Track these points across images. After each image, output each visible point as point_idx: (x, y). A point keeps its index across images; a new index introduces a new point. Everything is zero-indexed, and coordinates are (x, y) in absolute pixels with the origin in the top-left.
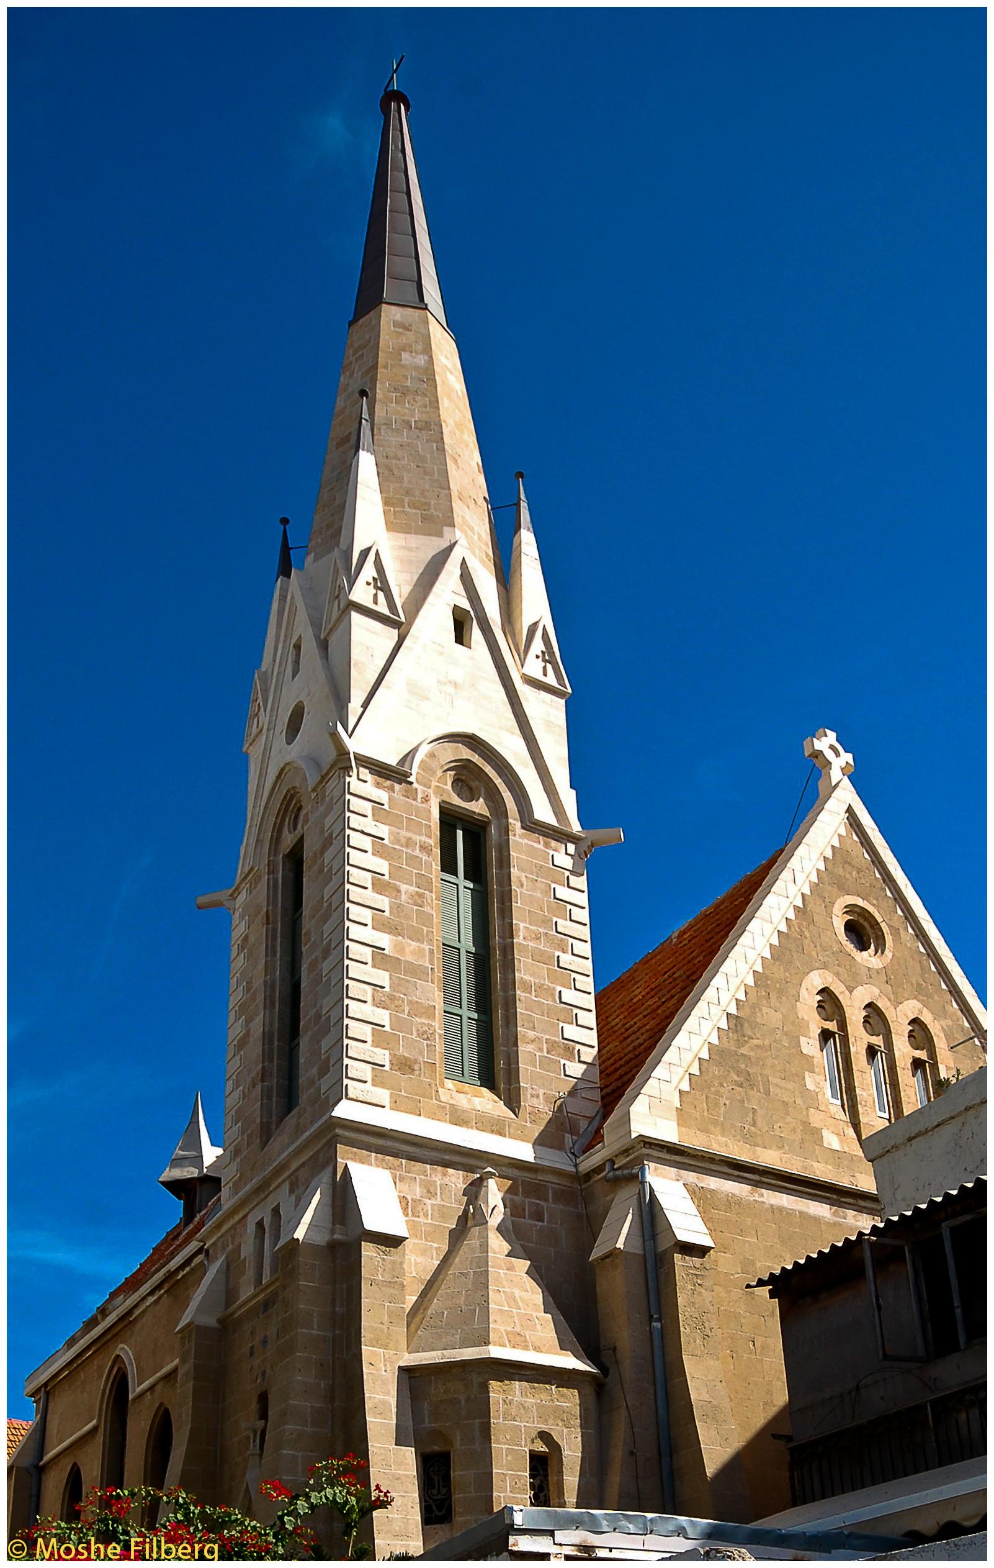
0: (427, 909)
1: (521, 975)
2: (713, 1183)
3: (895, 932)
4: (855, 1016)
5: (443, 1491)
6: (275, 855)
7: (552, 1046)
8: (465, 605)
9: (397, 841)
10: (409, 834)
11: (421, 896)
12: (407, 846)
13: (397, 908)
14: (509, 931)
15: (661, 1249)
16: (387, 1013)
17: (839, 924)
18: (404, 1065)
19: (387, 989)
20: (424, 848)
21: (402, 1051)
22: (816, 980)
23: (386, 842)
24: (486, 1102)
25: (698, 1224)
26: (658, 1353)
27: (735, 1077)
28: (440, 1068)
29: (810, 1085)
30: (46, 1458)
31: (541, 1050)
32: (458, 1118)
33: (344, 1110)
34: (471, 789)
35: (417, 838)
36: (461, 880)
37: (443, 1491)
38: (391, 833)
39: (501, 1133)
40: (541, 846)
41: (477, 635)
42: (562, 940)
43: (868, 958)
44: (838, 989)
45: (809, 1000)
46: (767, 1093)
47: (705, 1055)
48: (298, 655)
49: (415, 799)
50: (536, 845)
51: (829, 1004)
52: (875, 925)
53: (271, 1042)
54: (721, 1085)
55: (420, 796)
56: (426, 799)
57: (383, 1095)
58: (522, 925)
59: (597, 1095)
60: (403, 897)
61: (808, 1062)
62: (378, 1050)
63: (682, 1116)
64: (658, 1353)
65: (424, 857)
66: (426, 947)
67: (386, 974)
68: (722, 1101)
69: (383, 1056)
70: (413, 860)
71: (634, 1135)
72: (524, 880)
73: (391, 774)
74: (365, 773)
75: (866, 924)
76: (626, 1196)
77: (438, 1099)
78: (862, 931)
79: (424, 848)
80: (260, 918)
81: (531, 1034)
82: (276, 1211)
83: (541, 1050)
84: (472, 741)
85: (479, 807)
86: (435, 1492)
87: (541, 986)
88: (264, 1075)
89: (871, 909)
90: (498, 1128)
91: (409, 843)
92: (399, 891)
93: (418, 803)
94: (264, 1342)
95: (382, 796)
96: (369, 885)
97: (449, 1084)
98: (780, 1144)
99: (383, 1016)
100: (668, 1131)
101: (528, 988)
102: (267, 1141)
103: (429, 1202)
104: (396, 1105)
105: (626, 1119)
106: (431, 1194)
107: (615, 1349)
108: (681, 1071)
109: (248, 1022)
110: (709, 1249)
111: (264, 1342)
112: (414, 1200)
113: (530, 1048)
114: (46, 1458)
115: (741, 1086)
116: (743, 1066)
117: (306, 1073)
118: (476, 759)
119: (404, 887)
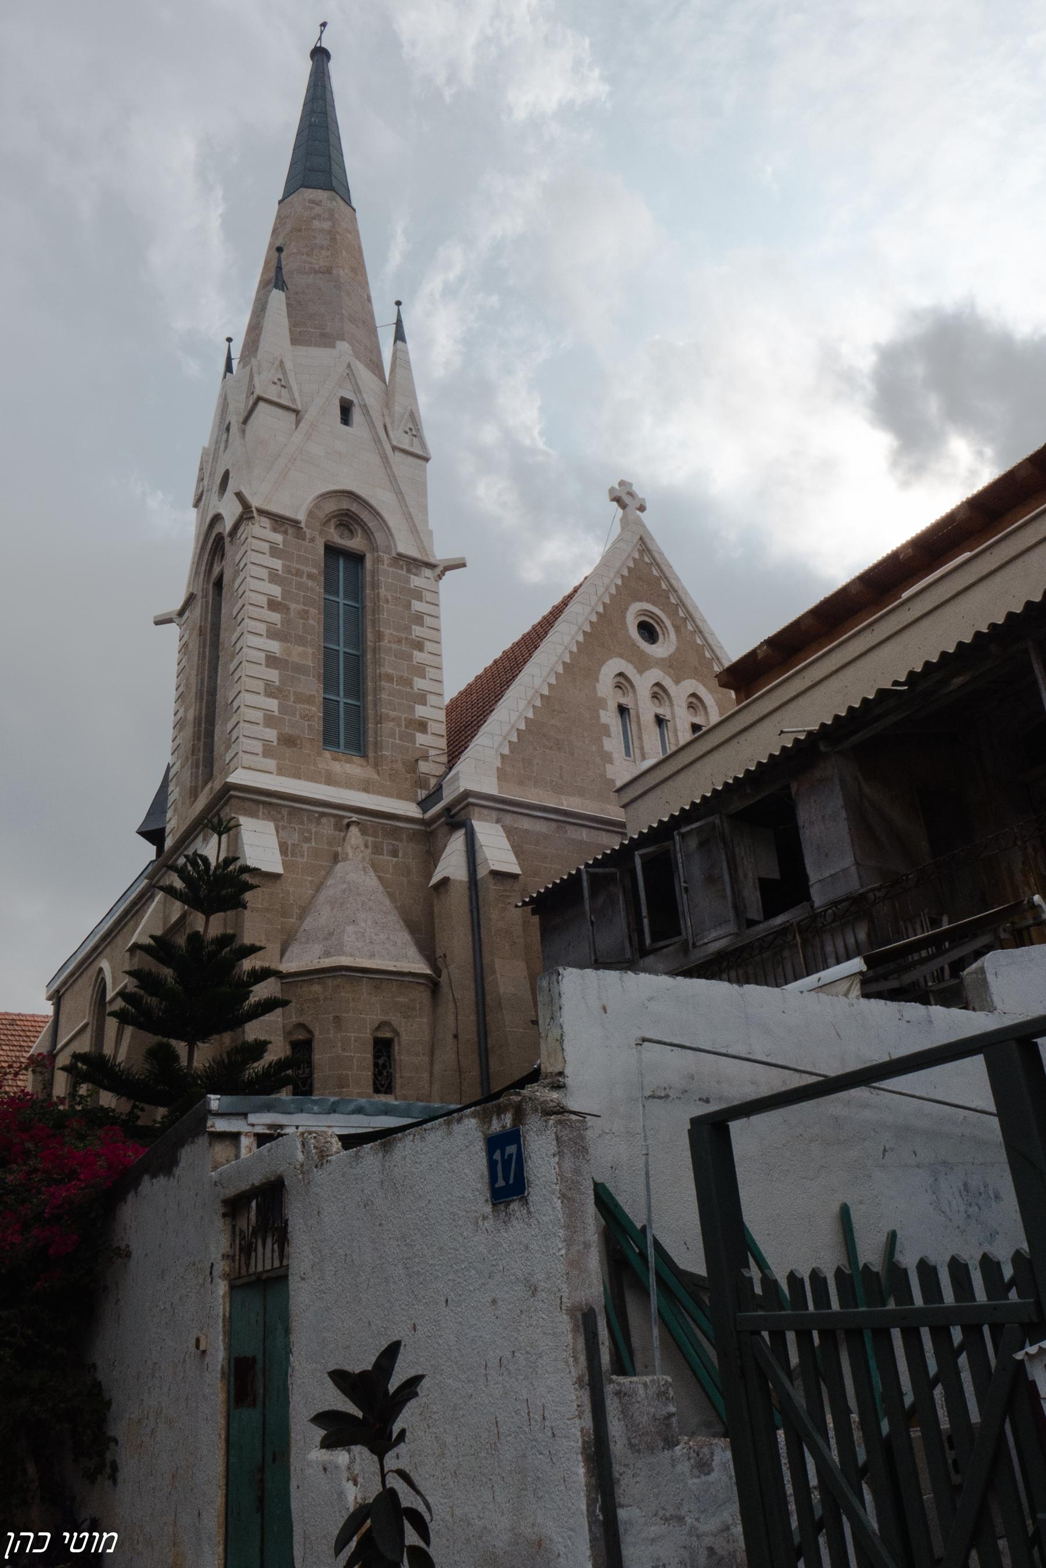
0: (311, 622)
2: (526, 824)
5: (307, 1071)
6: (208, 583)
9: (289, 572)
10: (298, 566)
11: (307, 612)
12: (296, 575)
18: (288, 741)
19: (277, 684)
20: (310, 576)
21: (286, 730)
23: (280, 573)
24: (355, 768)
27: (546, 743)
30: (59, 1046)
31: (399, 725)
32: (330, 780)
33: (238, 777)
34: (351, 531)
35: (302, 568)
37: (307, 1071)
38: (284, 566)
39: (366, 790)
40: (404, 572)
42: (419, 642)
47: (523, 727)
49: (304, 540)
50: (400, 571)
53: (200, 725)
54: (535, 749)
55: (308, 537)
56: (312, 540)
57: (271, 764)
58: (387, 632)
59: (444, 759)
60: (292, 614)
61: (606, 730)
62: (268, 730)
63: (502, 775)
65: (310, 583)
66: (310, 650)
67: (276, 672)
68: (535, 762)
69: (271, 735)
71: (462, 790)
72: (389, 597)
74: (266, 522)
79: (310, 576)
80: (196, 632)
83: (399, 725)
84: (351, 495)
85: (355, 543)
86: (301, 1072)
87: (401, 678)
88: (194, 750)
91: (298, 573)
92: (288, 609)
93: (306, 543)
95: (278, 538)
96: (266, 606)
97: (327, 754)
98: (581, 792)
100: (489, 786)
101: (390, 678)
102: (194, 801)
103: (306, 846)
104: (281, 771)
105: (456, 777)
106: (307, 840)
107: (445, 955)
108: (500, 738)
109: (186, 711)
110: (514, 877)
112: (293, 845)
113: (391, 724)
114: (59, 1046)
115: (551, 748)
118: (354, 508)
119: (293, 606)
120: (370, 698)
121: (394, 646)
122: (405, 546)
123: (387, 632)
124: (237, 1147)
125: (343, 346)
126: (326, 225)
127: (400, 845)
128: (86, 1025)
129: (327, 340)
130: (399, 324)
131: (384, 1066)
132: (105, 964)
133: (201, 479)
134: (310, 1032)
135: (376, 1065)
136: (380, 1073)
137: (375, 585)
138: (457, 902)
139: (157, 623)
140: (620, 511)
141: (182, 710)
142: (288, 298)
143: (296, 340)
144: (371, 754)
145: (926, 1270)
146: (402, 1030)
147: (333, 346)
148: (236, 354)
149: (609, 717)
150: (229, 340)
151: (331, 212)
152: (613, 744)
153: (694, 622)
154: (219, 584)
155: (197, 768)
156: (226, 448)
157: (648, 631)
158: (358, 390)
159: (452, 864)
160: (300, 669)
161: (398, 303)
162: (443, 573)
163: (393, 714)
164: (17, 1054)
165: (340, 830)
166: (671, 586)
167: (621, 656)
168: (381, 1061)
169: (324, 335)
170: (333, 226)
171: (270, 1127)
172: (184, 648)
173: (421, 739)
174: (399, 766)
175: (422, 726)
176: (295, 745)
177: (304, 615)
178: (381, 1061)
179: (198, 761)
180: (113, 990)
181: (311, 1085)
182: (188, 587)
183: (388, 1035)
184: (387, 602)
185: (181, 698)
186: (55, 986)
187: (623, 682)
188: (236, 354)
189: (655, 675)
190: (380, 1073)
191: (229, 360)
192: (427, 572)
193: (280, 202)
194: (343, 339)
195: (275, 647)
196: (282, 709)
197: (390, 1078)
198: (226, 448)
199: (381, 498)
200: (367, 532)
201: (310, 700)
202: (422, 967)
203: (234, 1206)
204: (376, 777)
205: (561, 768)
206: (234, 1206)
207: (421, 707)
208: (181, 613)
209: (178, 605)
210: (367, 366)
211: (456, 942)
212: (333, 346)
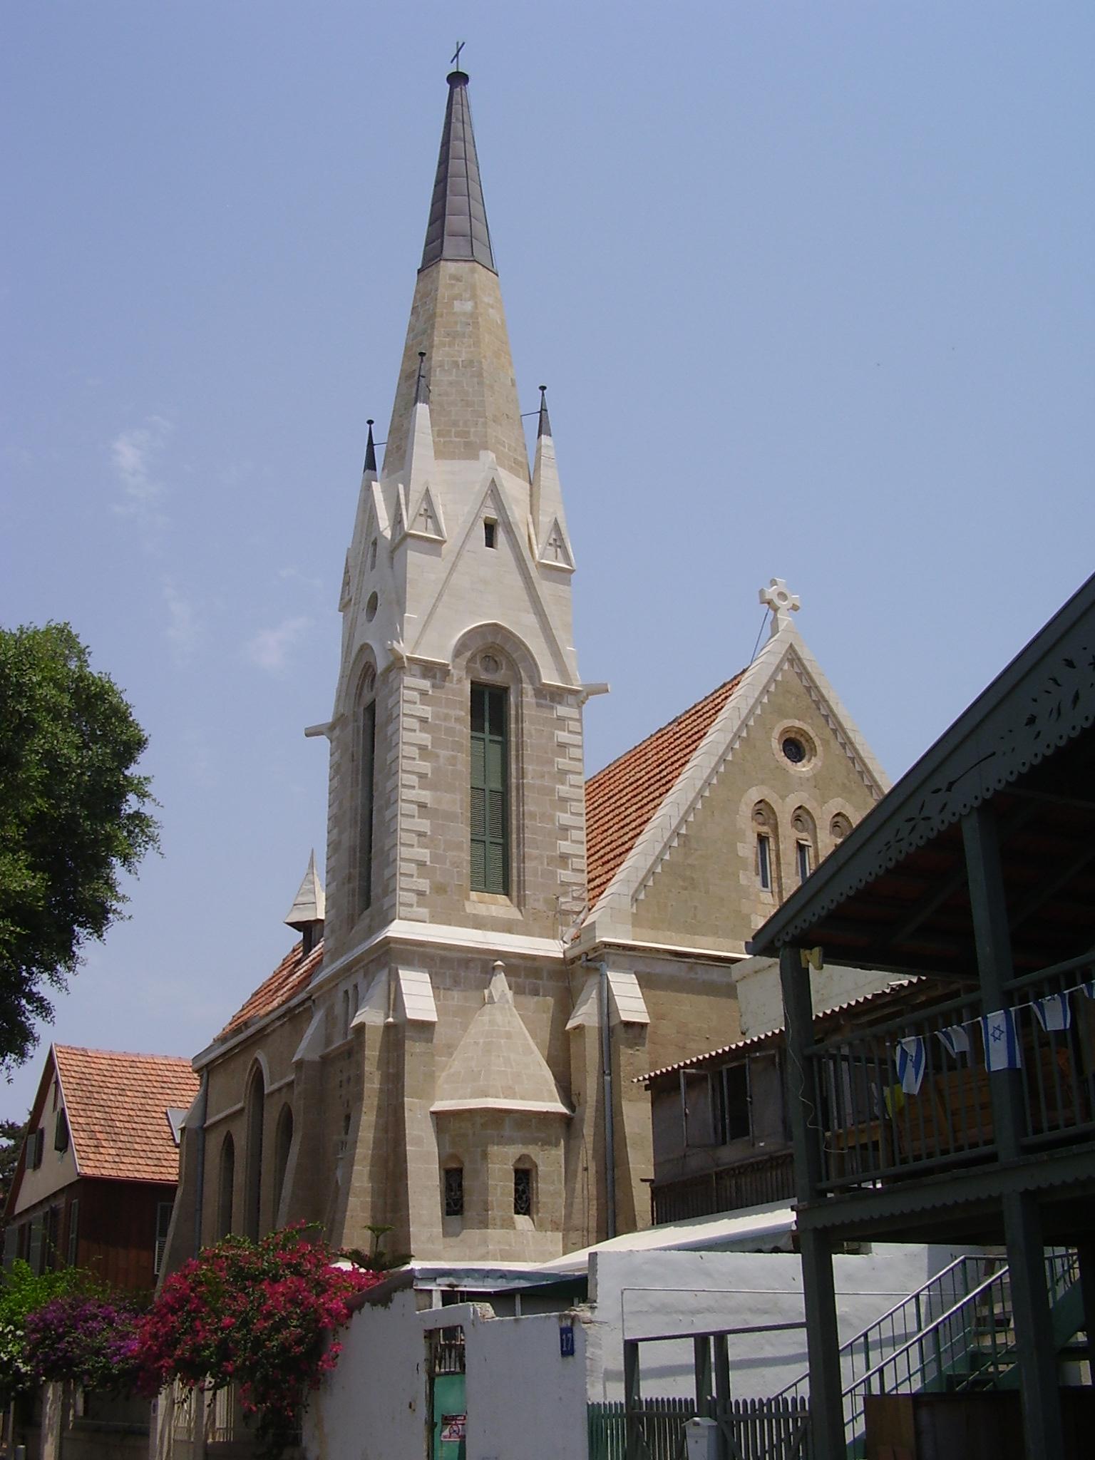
0: (459, 767)
1: (529, 807)
3: (826, 743)
4: (785, 815)
7: (551, 860)
8: (493, 515)
12: (445, 720)
13: (436, 770)
14: (522, 773)
15: (612, 1024)
16: (427, 851)
17: (776, 746)
18: (439, 889)
20: (457, 719)
22: (754, 795)
24: (499, 906)
25: (640, 1005)
26: (607, 1097)
28: (466, 883)
29: (743, 881)
32: (479, 923)
36: (487, 736)
39: (510, 931)
41: (501, 536)
43: (803, 768)
44: (773, 799)
45: (746, 809)
46: (707, 892)
48: (375, 550)
51: (763, 810)
52: (809, 740)
56: (460, 681)
58: (530, 768)
64: (607, 1097)
65: (458, 727)
69: (424, 884)
70: (449, 731)
73: (430, 670)
75: (802, 740)
76: (593, 980)
77: (464, 910)
78: (795, 748)
79: (457, 719)
81: (535, 852)
82: (356, 987)
89: (805, 727)
90: (508, 927)
91: (446, 718)
92: (438, 756)
94: (349, 1079)
99: (424, 854)
101: (533, 815)
110: (643, 1026)
111: (349, 1079)
116: (688, 873)
117: (376, 891)
119: (443, 753)
120: (514, 836)
121: (538, 782)
122: (549, 678)
123: (529, 768)
124: (431, 1298)
125: (488, 457)
126: (469, 306)
127: (539, 982)
128: (242, 1110)
129: (470, 450)
130: (543, 410)
131: (524, 1192)
132: (261, 1055)
133: (346, 583)
134: (461, 1162)
135: (516, 1191)
136: (520, 1198)
137: (519, 719)
138: (591, 1049)
139: (307, 735)
140: (771, 612)
141: (335, 831)
142: (431, 411)
143: (440, 454)
144: (514, 894)
145: (737, 1402)
146: (539, 1162)
147: (476, 457)
148: (381, 436)
149: (748, 849)
150: (370, 422)
151: (473, 287)
152: (749, 879)
153: (845, 733)
154: (371, 709)
155: (354, 895)
156: (373, 567)
157: (795, 748)
158: (500, 507)
159: (586, 1014)
160: (450, 816)
161: (543, 388)
162: (587, 698)
163: (535, 852)
164: (143, 1101)
165: (487, 973)
166: (823, 696)
167: (763, 782)
168: (521, 1188)
169: (467, 444)
170: (476, 306)
171: (449, 1286)
172: (336, 769)
173: (565, 875)
174: (540, 906)
175: (564, 858)
176: (445, 892)
177: (452, 761)
178: (521, 1188)
179: (354, 890)
180: (272, 1083)
181: (462, 1206)
182: (337, 707)
183: (527, 1166)
184: (531, 736)
185: (335, 820)
186: (205, 1061)
187: (763, 810)
188: (381, 436)
189: (793, 801)
190: (520, 1198)
191: (371, 445)
192: (571, 699)
193: (419, 271)
194: (486, 449)
195: (426, 796)
196: (435, 858)
197: (528, 1201)
198: (373, 567)
199: (523, 626)
200: (512, 665)
201: (459, 847)
202: (559, 1107)
203: (430, 1334)
204: (520, 917)
205: (696, 908)
206: (430, 1334)
207: (562, 815)
208: (332, 727)
209: (328, 718)
210: (511, 470)
211: (590, 1087)
212: (476, 457)
